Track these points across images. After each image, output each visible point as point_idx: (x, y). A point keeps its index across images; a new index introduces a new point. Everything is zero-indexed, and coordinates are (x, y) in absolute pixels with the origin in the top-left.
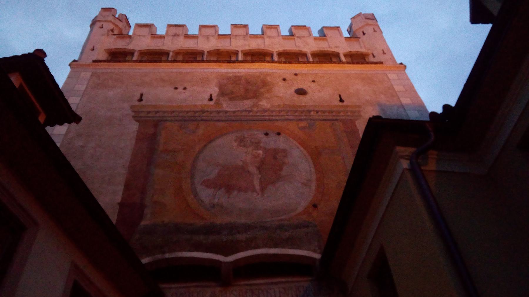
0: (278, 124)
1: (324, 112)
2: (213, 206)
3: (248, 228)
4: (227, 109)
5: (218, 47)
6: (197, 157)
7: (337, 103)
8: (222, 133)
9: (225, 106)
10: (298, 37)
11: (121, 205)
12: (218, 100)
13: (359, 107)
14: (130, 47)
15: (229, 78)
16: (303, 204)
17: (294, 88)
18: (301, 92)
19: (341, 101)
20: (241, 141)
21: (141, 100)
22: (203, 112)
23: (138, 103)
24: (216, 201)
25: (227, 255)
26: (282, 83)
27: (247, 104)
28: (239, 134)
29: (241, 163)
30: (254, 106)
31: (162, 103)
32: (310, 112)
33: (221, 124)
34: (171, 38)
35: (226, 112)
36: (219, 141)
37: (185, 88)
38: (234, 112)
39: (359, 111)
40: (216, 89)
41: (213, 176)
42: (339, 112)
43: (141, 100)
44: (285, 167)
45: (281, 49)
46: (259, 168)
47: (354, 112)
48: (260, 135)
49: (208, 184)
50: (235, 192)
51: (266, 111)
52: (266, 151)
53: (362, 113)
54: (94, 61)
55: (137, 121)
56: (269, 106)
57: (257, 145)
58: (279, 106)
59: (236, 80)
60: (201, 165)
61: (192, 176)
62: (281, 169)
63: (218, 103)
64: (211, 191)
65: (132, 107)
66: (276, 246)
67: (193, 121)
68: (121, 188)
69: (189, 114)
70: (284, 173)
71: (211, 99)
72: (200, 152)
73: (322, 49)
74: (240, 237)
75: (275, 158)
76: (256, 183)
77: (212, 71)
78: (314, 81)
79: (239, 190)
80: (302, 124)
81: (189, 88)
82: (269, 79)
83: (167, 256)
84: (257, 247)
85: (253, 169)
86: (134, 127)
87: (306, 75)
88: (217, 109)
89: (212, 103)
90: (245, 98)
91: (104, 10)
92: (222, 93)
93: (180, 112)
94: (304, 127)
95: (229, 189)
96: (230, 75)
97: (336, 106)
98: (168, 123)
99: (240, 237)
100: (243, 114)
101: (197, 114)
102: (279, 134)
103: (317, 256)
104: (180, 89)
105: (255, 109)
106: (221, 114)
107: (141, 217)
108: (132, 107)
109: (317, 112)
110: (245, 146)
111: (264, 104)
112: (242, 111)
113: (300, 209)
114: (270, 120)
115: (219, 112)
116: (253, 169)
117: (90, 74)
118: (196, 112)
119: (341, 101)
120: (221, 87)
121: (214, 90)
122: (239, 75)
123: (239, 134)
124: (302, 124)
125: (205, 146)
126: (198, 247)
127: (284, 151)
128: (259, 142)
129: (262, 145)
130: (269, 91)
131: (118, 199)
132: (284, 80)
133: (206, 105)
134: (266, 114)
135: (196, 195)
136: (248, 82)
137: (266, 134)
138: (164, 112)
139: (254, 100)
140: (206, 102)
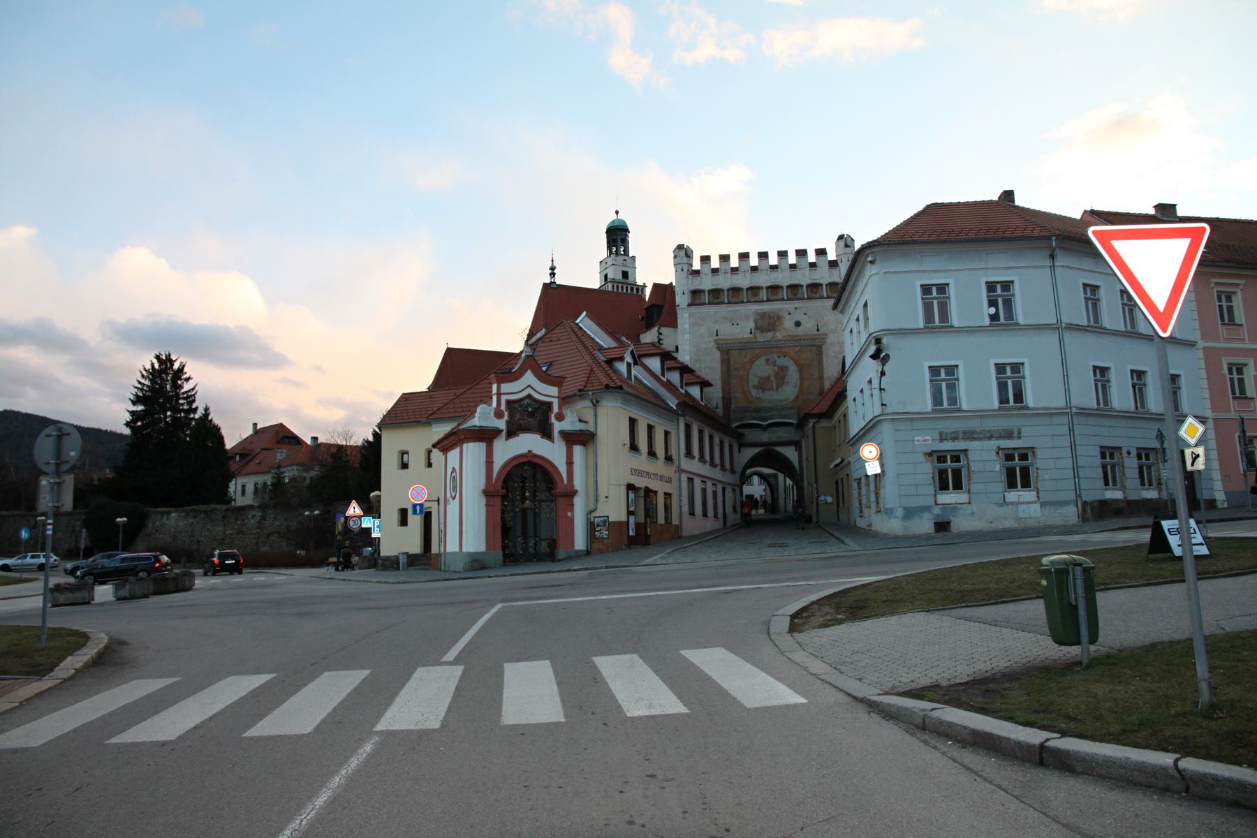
0: (785, 350)
1: (808, 340)
2: (757, 398)
3: (771, 409)
4: (760, 340)
5: (751, 283)
6: (748, 372)
7: (816, 332)
8: (758, 357)
9: (758, 338)
10: (800, 269)
11: (723, 398)
12: (755, 333)
13: (826, 334)
14: (702, 287)
15: (759, 314)
16: (793, 397)
17: (794, 321)
18: (798, 324)
19: (818, 330)
20: (767, 360)
21: (717, 335)
22: (748, 342)
23: (717, 338)
24: (758, 396)
25: (764, 421)
26: (788, 317)
27: (770, 335)
28: (766, 357)
29: (767, 375)
30: (774, 337)
31: (728, 337)
32: (801, 340)
33: (758, 351)
34: (723, 275)
35: (760, 342)
36: (758, 362)
37: (737, 324)
38: (764, 342)
39: (825, 338)
40: (753, 324)
41: (756, 383)
42: (815, 339)
43: (717, 335)
44: (787, 377)
45: (789, 283)
46: (775, 377)
47: (822, 339)
48: (775, 357)
49: (756, 387)
50: (766, 392)
51: (778, 341)
52: (779, 367)
53: (827, 340)
54: (689, 305)
55: (720, 350)
56: (781, 337)
57: (774, 364)
58: (785, 337)
59: (763, 315)
60: (751, 377)
61: (748, 384)
62: (785, 378)
63: (755, 336)
64: (756, 391)
65: (715, 341)
66: (781, 418)
67: (744, 349)
68: (721, 390)
69: (743, 344)
70: (786, 380)
71: (751, 333)
72: (750, 369)
73: (813, 282)
74: (769, 414)
75: (782, 371)
76: (774, 386)
77: (749, 308)
78: (805, 314)
79: (768, 390)
80: (796, 349)
81: (740, 325)
82: (781, 314)
83: (745, 422)
84: (775, 419)
85: (773, 378)
86: (718, 354)
87: (801, 308)
88: (756, 341)
89: (752, 336)
90: (769, 331)
91: (680, 247)
92: (757, 328)
93: (738, 343)
94: (797, 351)
95: (763, 390)
96: (760, 311)
97: (815, 335)
98: (733, 351)
99: (769, 414)
100: (769, 343)
101: (746, 344)
102: (785, 356)
103: (795, 422)
104: (735, 324)
105: (774, 340)
106: (757, 344)
107: (731, 404)
108: (715, 341)
109: (804, 340)
110: (770, 364)
111: (778, 335)
112: (768, 341)
113: (791, 400)
114: (780, 347)
115: (756, 342)
116: (773, 378)
117: (687, 315)
118: (745, 343)
119: (818, 330)
120: (756, 322)
121: (752, 325)
122: (765, 311)
123: (766, 357)
124: (796, 349)
125: (751, 366)
126: (754, 419)
127: (787, 367)
128: (775, 362)
129: (777, 363)
130: (781, 324)
131: (721, 395)
132: (789, 313)
133: (749, 338)
134: (779, 343)
135: (750, 393)
136: (770, 317)
137: (779, 357)
138: (730, 344)
139: (773, 332)
140: (747, 335)
